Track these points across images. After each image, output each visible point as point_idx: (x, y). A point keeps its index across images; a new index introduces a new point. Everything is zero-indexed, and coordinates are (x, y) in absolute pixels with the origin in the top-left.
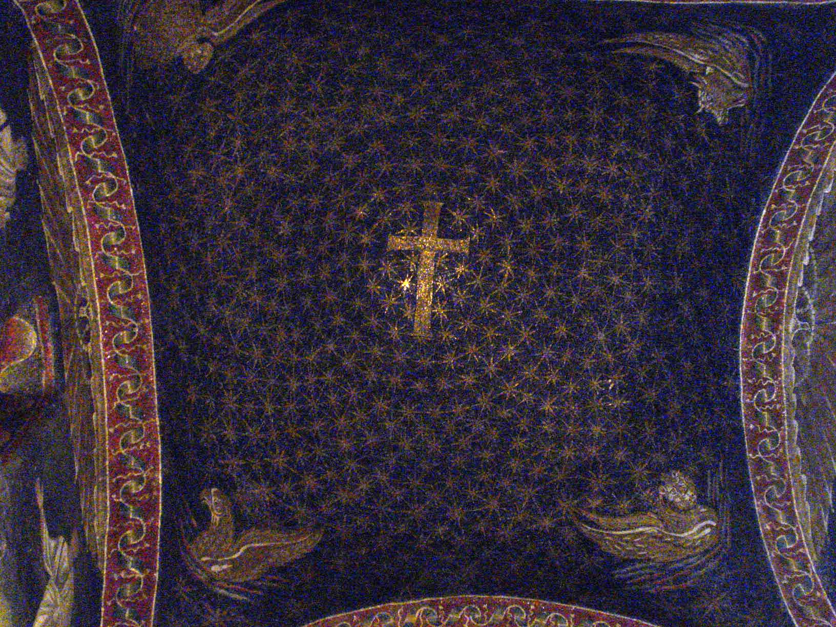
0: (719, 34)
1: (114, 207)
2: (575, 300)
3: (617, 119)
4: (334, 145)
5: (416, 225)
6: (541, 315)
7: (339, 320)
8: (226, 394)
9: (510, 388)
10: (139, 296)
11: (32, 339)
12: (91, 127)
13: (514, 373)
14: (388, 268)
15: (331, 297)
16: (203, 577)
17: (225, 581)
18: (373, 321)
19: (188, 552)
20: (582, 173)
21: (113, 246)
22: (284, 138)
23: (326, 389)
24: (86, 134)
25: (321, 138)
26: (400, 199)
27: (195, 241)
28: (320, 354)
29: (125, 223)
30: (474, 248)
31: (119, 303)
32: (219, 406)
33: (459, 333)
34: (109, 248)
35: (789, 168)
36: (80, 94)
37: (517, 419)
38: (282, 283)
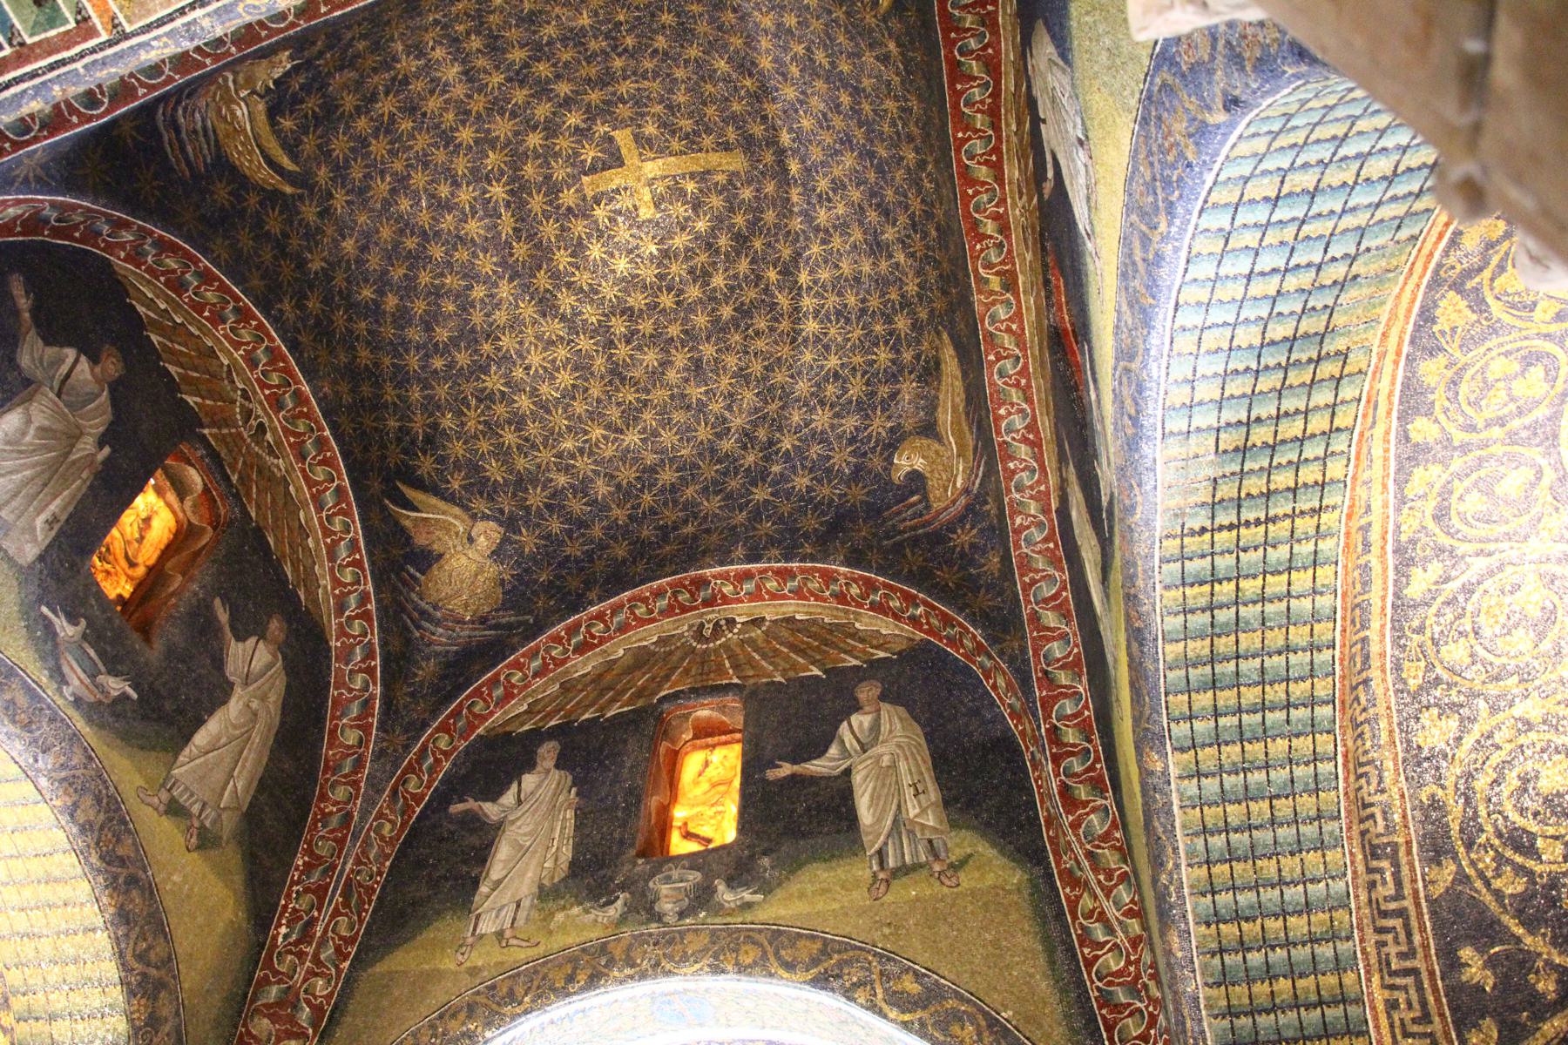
0: (195, 131)
2: (621, 18)
6: (661, 42)
7: (743, 266)
9: (766, 63)
11: (704, 713)
12: (544, 659)
15: (718, 281)
16: (963, 501)
19: (939, 513)
20: (466, 73)
23: (815, 283)
24: (552, 658)
25: (551, 343)
27: (667, 476)
28: (781, 290)
32: (822, 438)
34: (651, 612)
35: (264, 33)
38: (708, 350)
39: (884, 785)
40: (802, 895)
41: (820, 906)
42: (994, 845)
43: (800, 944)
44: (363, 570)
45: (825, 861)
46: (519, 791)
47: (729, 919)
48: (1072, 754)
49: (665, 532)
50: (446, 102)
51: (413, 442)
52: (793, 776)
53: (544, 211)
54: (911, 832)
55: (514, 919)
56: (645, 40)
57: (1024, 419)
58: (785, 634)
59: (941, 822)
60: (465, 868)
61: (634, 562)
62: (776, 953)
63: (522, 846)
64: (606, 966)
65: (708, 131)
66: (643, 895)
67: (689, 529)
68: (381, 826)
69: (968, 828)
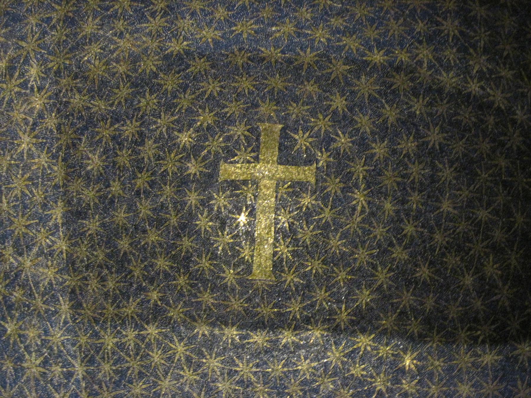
2: (438, 237)
3: (475, 31)
4: (149, 65)
5: (253, 151)
6: (399, 254)
7: (162, 263)
8: (27, 357)
9: (364, 342)
13: (370, 322)
14: (221, 201)
15: (153, 237)
18: (205, 263)
20: (440, 91)
22: (89, 61)
23: (149, 346)
26: (231, 121)
30: (322, 176)
32: (19, 371)
33: (305, 276)
37: (372, 377)
38: (92, 225)
50: (420, 63)
53: (267, 85)
56: (406, 241)
65: (294, 253)
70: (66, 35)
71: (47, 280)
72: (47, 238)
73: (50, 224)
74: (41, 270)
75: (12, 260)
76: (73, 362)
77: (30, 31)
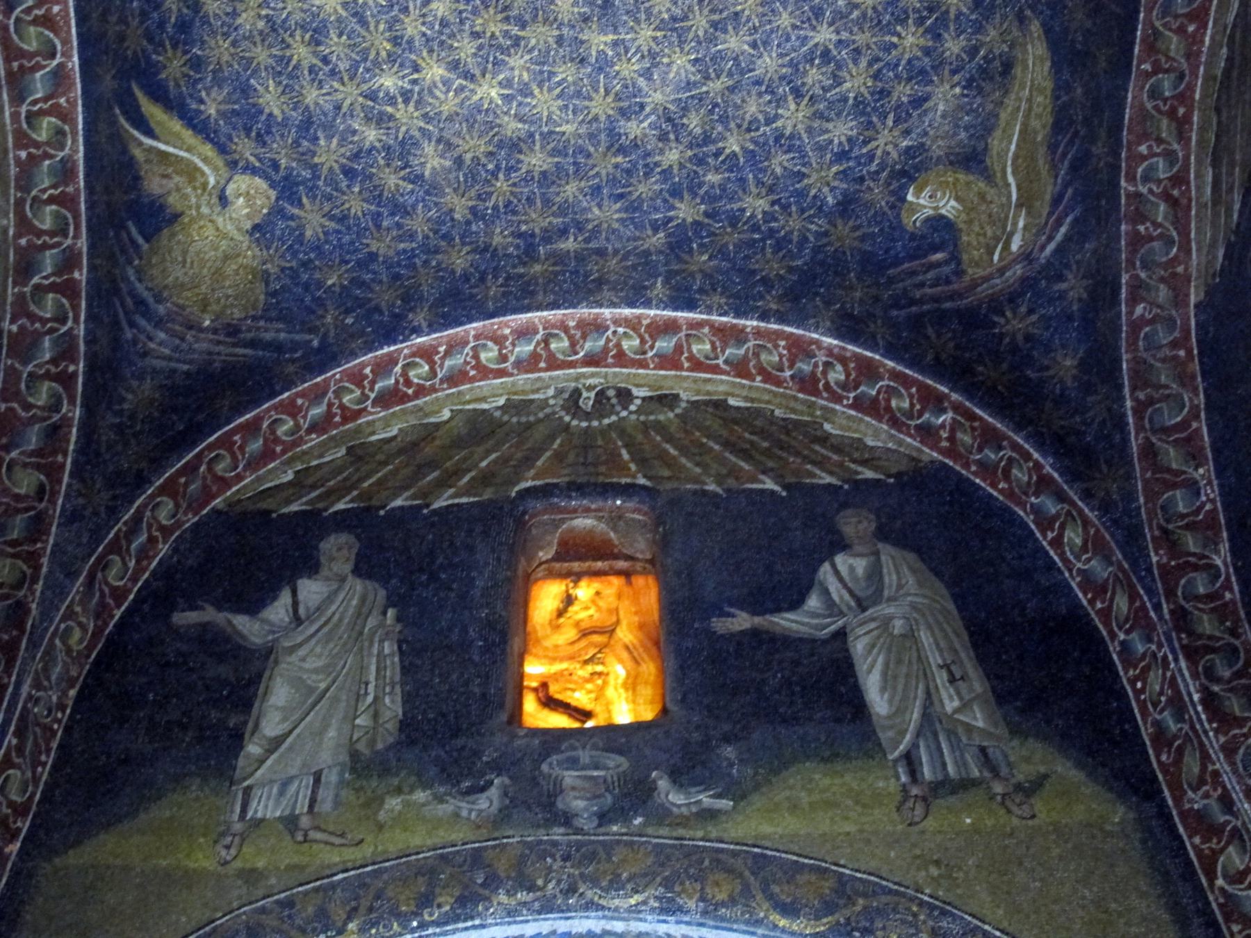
1: (443, 358)
10: (572, 324)
11: (583, 523)
12: (330, 405)
16: (1018, 270)
17: (1038, 235)
19: (974, 284)
21: (500, 353)
24: (342, 407)
27: (537, 160)
29: (467, 343)
31: (582, 347)
34: (503, 358)
36: (281, 430)
39: (899, 662)
40: (794, 808)
41: (825, 827)
42: (1080, 765)
43: (801, 879)
44: (76, 217)
45: (824, 760)
46: (295, 604)
47: (681, 832)
48: (1214, 650)
49: (529, 246)
51: (161, 25)
52: (755, 633)
54: (951, 733)
55: (313, 802)
57: (1172, 165)
58: (715, 425)
59: (996, 725)
60: (214, 715)
61: (482, 279)
62: (765, 890)
63: (311, 690)
64: (483, 885)
66: (534, 782)
67: (569, 244)
68: (68, 630)
69: (1037, 736)
70: (340, 36)
71: (689, 66)
72: (630, 60)
73: (610, 53)
74: (672, 75)
75: (645, 124)
76: (812, 43)
77: (327, 98)
